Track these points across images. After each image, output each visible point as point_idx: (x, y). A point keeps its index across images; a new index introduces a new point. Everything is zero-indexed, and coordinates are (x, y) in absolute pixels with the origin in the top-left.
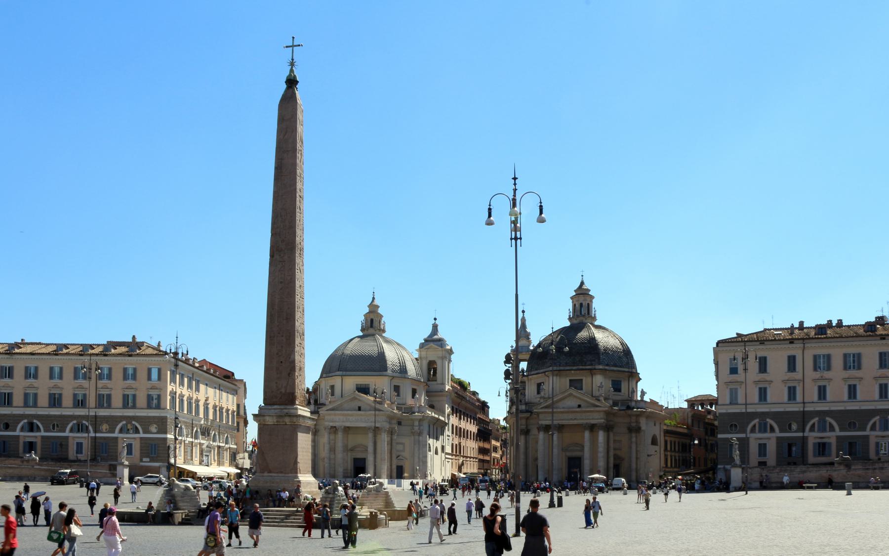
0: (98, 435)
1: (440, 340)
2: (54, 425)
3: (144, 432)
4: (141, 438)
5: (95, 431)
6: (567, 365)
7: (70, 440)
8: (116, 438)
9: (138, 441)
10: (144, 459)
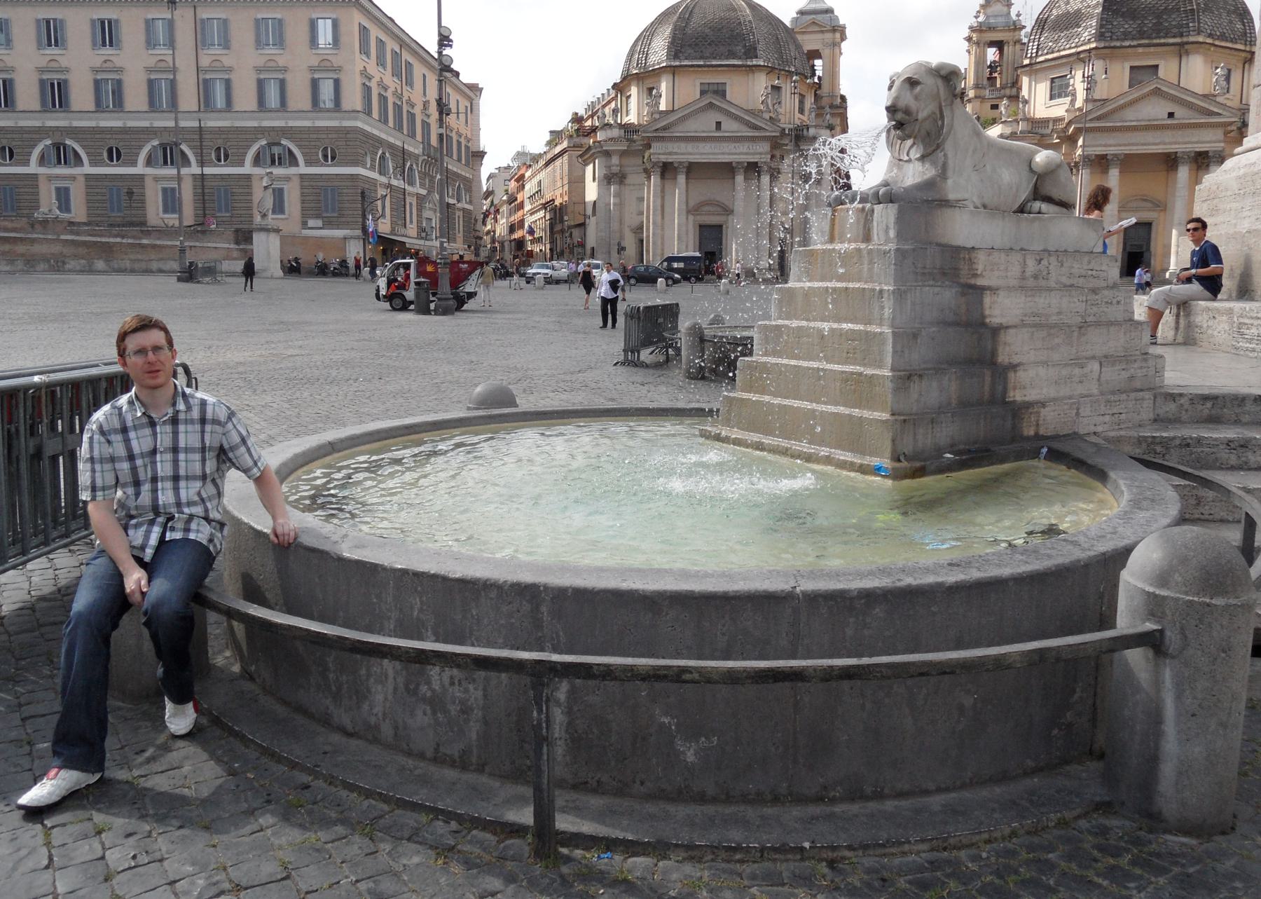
0: (208, 171)
1: (829, 11)
2: (110, 151)
3: (309, 163)
4: (302, 177)
5: (202, 164)
6: (1126, 36)
7: (149, 183)
8: (248, 177)
9: (296, 183)
10: (311, 223)
